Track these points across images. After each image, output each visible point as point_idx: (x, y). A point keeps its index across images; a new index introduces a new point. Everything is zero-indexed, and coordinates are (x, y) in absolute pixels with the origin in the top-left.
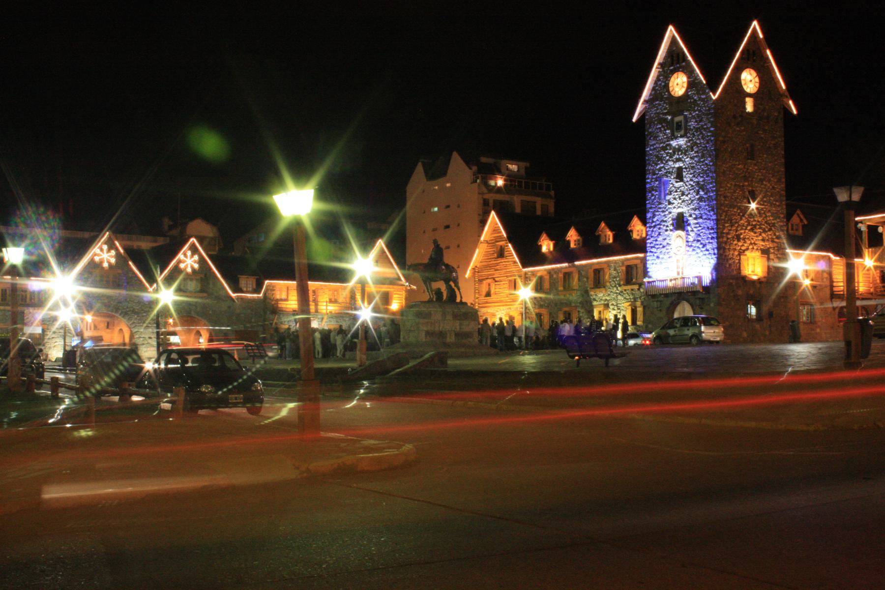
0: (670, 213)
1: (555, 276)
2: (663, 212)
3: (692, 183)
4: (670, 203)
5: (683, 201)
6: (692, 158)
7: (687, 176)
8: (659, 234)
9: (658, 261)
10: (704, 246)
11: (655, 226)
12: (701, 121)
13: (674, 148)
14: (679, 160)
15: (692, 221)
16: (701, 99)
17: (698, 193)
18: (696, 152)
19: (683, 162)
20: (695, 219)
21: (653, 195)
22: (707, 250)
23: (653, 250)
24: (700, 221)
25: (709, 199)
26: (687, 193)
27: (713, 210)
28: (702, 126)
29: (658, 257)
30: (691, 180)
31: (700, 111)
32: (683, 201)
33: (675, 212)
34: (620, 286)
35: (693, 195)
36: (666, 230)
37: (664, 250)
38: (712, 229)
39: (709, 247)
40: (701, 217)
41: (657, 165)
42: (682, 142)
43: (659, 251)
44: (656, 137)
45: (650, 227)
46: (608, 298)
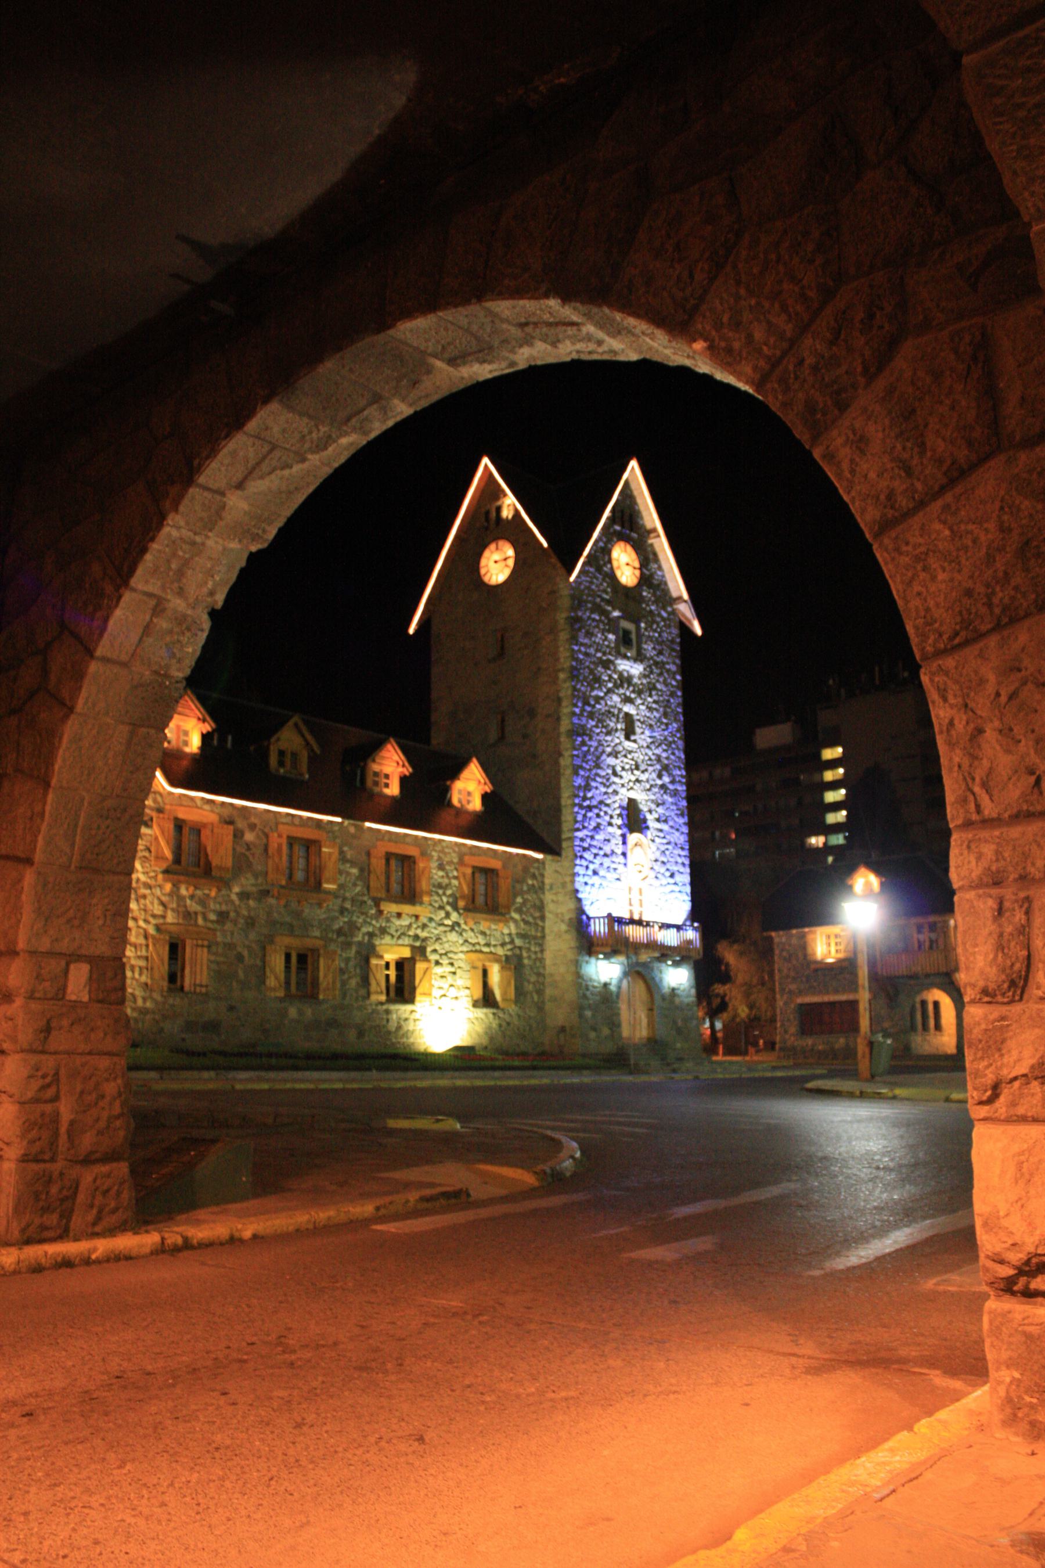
0: (615, 792)
1: (249, 837)
2: (605, 785)
3: (650, 753)
4: (615, 774)
5: (638, 781)
6: (650, 709)
7: (643, 736)
8: (597, 828)
9: (595, 880)
10: (672, 876)
11: (590, 808)
12: (660, 653)
13: (621, 674)
14: (627, 700)
15: (652, 824)
16: (659, 615)
17: (660, 776)
18: (655, 702)
19: (638, 708)
20: (658, 820)
21: (583, 743)
22: (675, 884)
23: (586, 855)
24: (665, 827)
25: (675, 794)
26: (643, 767)
27: (682, 815)
28: (663, 663)
29: (595, 873)
30: (648, 747)
31: (660, 635)
32: (638, 781)
33: (624, 795)
34: (456, 908)
35: (650, 775)
36: (610, 824)
37: (607, 862)
38: (682, 849)
39: (678, 878)
40: (666, 821)
41: (593, 689)
42: (635, 670)
43: (598, 861)
44: (589, 634)
45: (581, 807)
46: (423, 934)
